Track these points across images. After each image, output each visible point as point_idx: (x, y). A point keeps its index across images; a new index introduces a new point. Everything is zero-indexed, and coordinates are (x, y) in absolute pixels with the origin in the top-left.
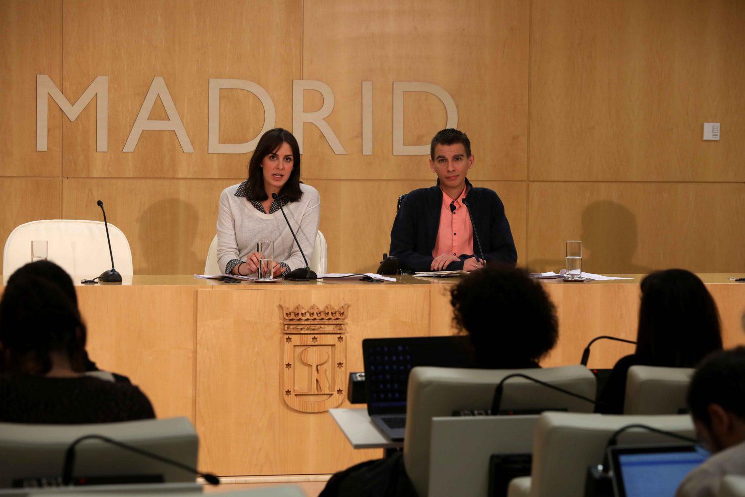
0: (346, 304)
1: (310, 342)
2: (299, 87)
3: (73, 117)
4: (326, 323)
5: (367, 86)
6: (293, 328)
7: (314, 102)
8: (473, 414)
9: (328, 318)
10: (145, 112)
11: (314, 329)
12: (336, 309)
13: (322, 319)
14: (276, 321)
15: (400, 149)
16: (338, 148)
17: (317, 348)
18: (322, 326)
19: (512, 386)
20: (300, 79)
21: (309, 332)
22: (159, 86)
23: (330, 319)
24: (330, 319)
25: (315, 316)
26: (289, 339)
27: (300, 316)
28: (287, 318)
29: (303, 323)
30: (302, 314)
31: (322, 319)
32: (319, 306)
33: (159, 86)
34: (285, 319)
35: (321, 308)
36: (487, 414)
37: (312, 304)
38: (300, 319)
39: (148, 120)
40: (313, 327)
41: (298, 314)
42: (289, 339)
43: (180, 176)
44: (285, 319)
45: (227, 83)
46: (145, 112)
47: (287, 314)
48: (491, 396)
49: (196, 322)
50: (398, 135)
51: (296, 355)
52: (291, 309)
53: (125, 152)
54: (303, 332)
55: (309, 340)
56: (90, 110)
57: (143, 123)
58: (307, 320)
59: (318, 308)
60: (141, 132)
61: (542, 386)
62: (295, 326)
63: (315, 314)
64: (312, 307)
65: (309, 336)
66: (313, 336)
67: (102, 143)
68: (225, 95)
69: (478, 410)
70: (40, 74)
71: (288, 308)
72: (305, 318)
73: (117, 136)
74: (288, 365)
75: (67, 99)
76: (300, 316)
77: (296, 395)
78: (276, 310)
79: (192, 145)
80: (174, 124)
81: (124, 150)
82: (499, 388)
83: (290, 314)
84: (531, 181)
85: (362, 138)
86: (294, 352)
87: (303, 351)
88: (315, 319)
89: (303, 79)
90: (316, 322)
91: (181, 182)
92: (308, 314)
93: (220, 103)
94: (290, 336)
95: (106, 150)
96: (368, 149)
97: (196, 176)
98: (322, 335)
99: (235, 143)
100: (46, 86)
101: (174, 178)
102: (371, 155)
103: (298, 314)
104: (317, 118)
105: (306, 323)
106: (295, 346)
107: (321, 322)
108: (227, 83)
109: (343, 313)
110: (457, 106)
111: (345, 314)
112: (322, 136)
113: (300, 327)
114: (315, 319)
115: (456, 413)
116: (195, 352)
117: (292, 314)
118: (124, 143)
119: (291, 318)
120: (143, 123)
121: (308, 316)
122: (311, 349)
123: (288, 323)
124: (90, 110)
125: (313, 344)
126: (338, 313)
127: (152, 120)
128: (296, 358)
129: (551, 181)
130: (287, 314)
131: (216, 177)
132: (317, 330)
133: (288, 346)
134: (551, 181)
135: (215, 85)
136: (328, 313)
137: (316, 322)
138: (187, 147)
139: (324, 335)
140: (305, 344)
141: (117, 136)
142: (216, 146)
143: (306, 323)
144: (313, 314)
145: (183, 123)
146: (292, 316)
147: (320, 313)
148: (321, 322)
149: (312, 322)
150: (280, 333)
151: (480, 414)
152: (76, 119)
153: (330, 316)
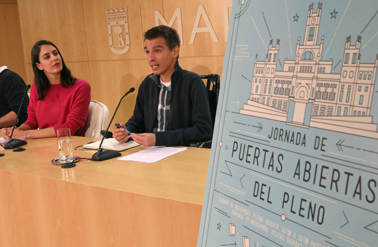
10: (196, 24)
43: (214, 55)
46: (196, 24)
57: (196, 30)
70: (156, 10)
80: (208, 29)
81: (190, 43)
91: (215, 58)
97: (221, 55)
101: (211, 56)
118: (189, 39)
120: (196, 30)
127: (200, 27)
138: (215, 40)
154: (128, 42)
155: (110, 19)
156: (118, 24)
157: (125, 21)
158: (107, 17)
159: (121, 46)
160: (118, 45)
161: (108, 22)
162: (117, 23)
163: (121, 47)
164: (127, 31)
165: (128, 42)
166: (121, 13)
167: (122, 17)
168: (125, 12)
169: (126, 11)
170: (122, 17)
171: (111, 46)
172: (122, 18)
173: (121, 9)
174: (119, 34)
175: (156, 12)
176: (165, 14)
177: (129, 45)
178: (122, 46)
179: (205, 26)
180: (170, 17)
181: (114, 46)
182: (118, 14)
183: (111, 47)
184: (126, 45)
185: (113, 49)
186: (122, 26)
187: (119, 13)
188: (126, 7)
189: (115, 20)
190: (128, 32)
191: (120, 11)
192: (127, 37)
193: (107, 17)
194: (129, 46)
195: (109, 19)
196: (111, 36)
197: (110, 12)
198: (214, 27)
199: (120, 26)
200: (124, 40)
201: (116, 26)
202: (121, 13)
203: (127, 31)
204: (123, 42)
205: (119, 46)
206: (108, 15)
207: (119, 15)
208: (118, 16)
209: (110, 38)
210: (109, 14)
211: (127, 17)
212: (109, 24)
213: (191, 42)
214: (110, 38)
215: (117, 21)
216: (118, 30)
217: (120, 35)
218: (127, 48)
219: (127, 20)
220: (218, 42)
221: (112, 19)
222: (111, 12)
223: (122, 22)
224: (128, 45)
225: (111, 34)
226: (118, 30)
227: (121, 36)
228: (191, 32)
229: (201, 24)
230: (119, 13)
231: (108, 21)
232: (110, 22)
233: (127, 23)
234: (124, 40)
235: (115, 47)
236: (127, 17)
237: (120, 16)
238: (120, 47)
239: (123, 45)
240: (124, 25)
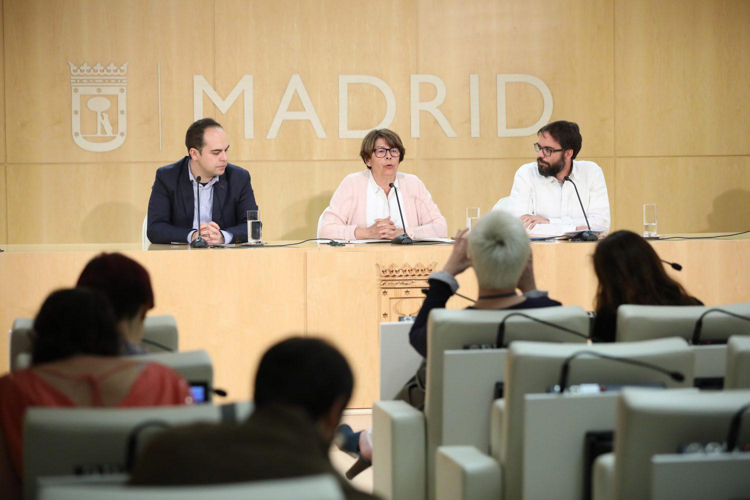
0: (433, 263)
1: (404, 295)
2: (416, 80)
3: (224, 112)
4: (417, 278)
5: (474, 79)
6: (389, 284)
7: (428, 93)
8: (480, 348)
9: (418, 274)
11: (406, 284)
12: (426, 266)
13: (414, 275)
14: (375, 278)
15: (504, 131)
16: (449, 131)
17: (409, 299)
18: (414, 281)
19: (516, 325)
20: (417, 74)
21: (402, 286)
22: (296, 83)
23: (420, 275)
24: (420, 275)
25: (408, 273)
26: (385, 292)
27: (394, 273)
28: (384, 275)
29: (397, 278)
30: (396, 271)
31: (414, 275)
32: (410, 264)
33: (296, 83)
34: (382, 276)
35: (413, 266)
36: (492, 347)
37: (405, 263)
38: (394, 276)
39: (287, 111)
40: (405, 282)
41: (392, 271)
43: (315, 158)
44: (382, 276)
45: (354, 79)
47: (383, 271)
48: (495, 333)
49: (305, 280)
50: (502, 118)
51: (392, 306)
52: (387, 268)
53: (268, 139)
54: (397, 286)
55: (402, 293)
56: (238, 104)
57: (283, 114)
58: (401, 276)
59: (409, 266)
60: (281, 122)
61: (542, 325)
62: (390, 282)
63: (407, 271)
64: (405, 266)
65: (402, 289)
66: (406, 290)
67: (249, 132)
68: (353, 89)
69: (484, 344)
71: (383, 267)
72: (399, 274)
73: (261, 127)
74: (385, 315)
75: (219, 94)
76: (394, 273)
78: (374, 267)
79: (325, 131)
80: (310, 114)
81: (268, 137)
82: (502, 326)
83: (386, 271)
84: (617, 157)
85: (470, 123)
86: (390, 304)
87: (397, 303)
88: (407, 275)
89: (418, 74)
90: (408, 278)
92: (401, 271)
93: (348, 96)
94: (386, 290)
95: (252, 137)
96: (475, 132)
98: (414, 289)
100: (201, 84)
102: (478, 137)
103: (392, 271)
104: (431, 107)
105: (400, 278)
106: (390, 298)
107: (413, 278)
108: (354, 79)
109: (431, 270)
110: (552, 95)
111: (433, 271)
112: (436, 122)
113: (394, 282)
114: (407, 275)
115: (466, 347)
116: (306, 305)
117: (388, 271)
118: (267, 132)
119: (386, 275)
121: (401, 273)
122: (404, 301)
123: (384, 279)
124: (238, 104)
125: (406, 297)
126: (426, 270)
128: (392, 309)
129: (635, 157)
130: (383, 271)
131: (346, 158)
132: (409, 284)
133: (385, 299)
134: (635, 157)
135: (344, 81)
136: (418, 270)
137: (408, 278)
138: (320, 133)
139: (415, 289)
140: (400, 297)
141: (261, 127)
143: (400, 278)
144: (405, 271)
145: (316, 111)
146: (388, 273)
147: (412, 270)
148: (413, 278)
149: (405, 278)
150: (378, 288)
151: (487, 348)
152: (227, 112)
153: (420, 272)
155: (78, 81)
156: (101, 93)
157: (121, 88)
158: (72, 78)
159: (103, 136)
161: (74, 88)
162: (99, 90)
163: (104, 137)
164: (122, 106)
165: (122, 126)
166: (112, 72)
167: (112, 81)
169: (124, 70)
170: (112, 80)
171: (77, 134)
172: (112, 83)
174: (102, 113)
177: (125, 134)
178: (106, 135)
181: (84, 136)
182: (102, 74)
184: (117, 134)
185: (80, 141)
187: (105, 72)
188: (124, 63)
189: (94, 84)
190: (125, 110)
191: (109, 68)
193: (72, 78)
194: (124, 137)
196: (79, 116)
197: (82, 68)
199: (107, 96)
200: (114, 124)
201: (95, 96)
202: (112, 72)
205: (99, 134)
206: (77, 74)
207: (106, 75)
212: (76, 91)
213: (273, 133)
214: (76, 121)
215: (98, 87)
216: (100, 105)
217: (104, 114)
218: (119, 141)
221: (85, 81)
224: (122, 134)
225: (79, 109)
227: (106, 116)
228: (273, 118)
229: (296, 105)
230: (105, 72)
231: (72, 84)
232: (77, 88)
233: (125, 93)
234: (114, 124)
235: (86, 137)
236: (123, 81)
237: (107, 78)
238: (101, 137)
239: (109, 133)
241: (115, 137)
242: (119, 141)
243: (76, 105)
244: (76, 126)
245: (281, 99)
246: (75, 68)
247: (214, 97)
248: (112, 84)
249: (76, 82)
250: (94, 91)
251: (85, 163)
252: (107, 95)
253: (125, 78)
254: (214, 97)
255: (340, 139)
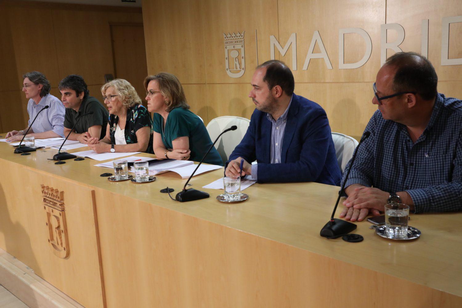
10: (311, 50)
42: (45, 208)
43: (327, 81)
57: (310, 56)
70: (271, 35)
77: (53, 244)
80: (323, 55)
94: (46, 206)
99: (352, 63)
101: (324, 83)
120: (310, 56)
127: (314, 53)
142: (342, 66)
154: (243, 66)
156: (235, 48)
158: (225, 41)
160: (234, 69)
161: (225, 46)
162: (234, 47)
164: (243, 55)
165: (243, 66)
166: (238, 37)
168: (242, 36)
173: (238, 33)
175: (272, 37)
176: (281, 39)
178: (238, 70)
179: (319, 52)
180: (285, 43)
183: (227, 71)
184: (241, 69)
185: (228, 72)
186: (239, 50)
189: (232, 44)
191: (237, 35)
192: (243, 61)
194: (244, 70)
195: (226, 43)
198: (328, 53)
199: (236, 50)
200: (240, 64)
201: (233, 50)
203: (243, 55)
204: (238, 66)
206: (226, 39)
208: (235, 40)
209: (227, 61)
210: (227, 38)
211: (243, 41)
214: (227, 61)
216: (234, 54)
217: (236, 59)
218: (243, 72)
219: (243, 45)
220: (332, 68)
222: (229, 36)
223: (238, 46)
226: (234, 54)
230: (236, 38)
231: (225, 44)
234: (240, 64)
239: (239, 69)
240: (240, 49)
241: (241, 70)
242: (243, 72)
243: (227, 56)
244: (227, 67)
245: (309, 47)
246: (225, 36)
247: (278, 47)
248: (238, 43)
249: (226, 43)
250: (232, 47)
251: (231, 84)
252: (237, 49)
253: (243, 40)
254: (278, 47)
255: (340, 69)
